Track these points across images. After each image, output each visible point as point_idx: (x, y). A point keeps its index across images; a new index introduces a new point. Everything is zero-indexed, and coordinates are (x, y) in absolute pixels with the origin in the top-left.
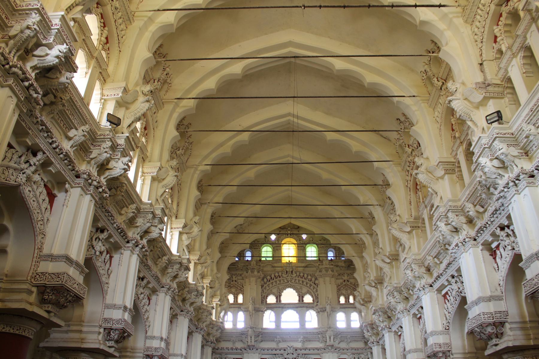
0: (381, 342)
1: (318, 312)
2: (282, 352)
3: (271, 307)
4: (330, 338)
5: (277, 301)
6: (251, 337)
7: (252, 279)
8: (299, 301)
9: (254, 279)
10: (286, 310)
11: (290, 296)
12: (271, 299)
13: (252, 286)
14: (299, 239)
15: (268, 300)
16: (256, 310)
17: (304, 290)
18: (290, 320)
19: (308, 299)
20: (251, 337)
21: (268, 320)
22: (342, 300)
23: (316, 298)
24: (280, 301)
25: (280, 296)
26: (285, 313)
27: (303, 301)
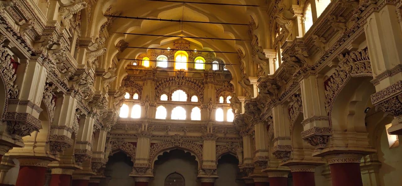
0: (250, 133)
1: (202, 108)
2: (169, 138)
3: (164, 103)
4: (210, 129)
5: (168, 99)
6: (145, 127)
7: (149, 81)
8: (188, 100)
9: (150, 81)
10: (175, 107)
11: (180, 95)
12: (164, 98)
13: (149, 88)
14: (190, 51)
15: (161, 98)
16: (150, 103)
17: (192, 92)
18: (179, 114)
19: (195, 99)
20: (145, 127)
21: (161, 113)
22: (221, 100)
23: (201, 98)
24: (171, 99)
25: (171, 95)
26: (174, 109)
27: (190, 100)
